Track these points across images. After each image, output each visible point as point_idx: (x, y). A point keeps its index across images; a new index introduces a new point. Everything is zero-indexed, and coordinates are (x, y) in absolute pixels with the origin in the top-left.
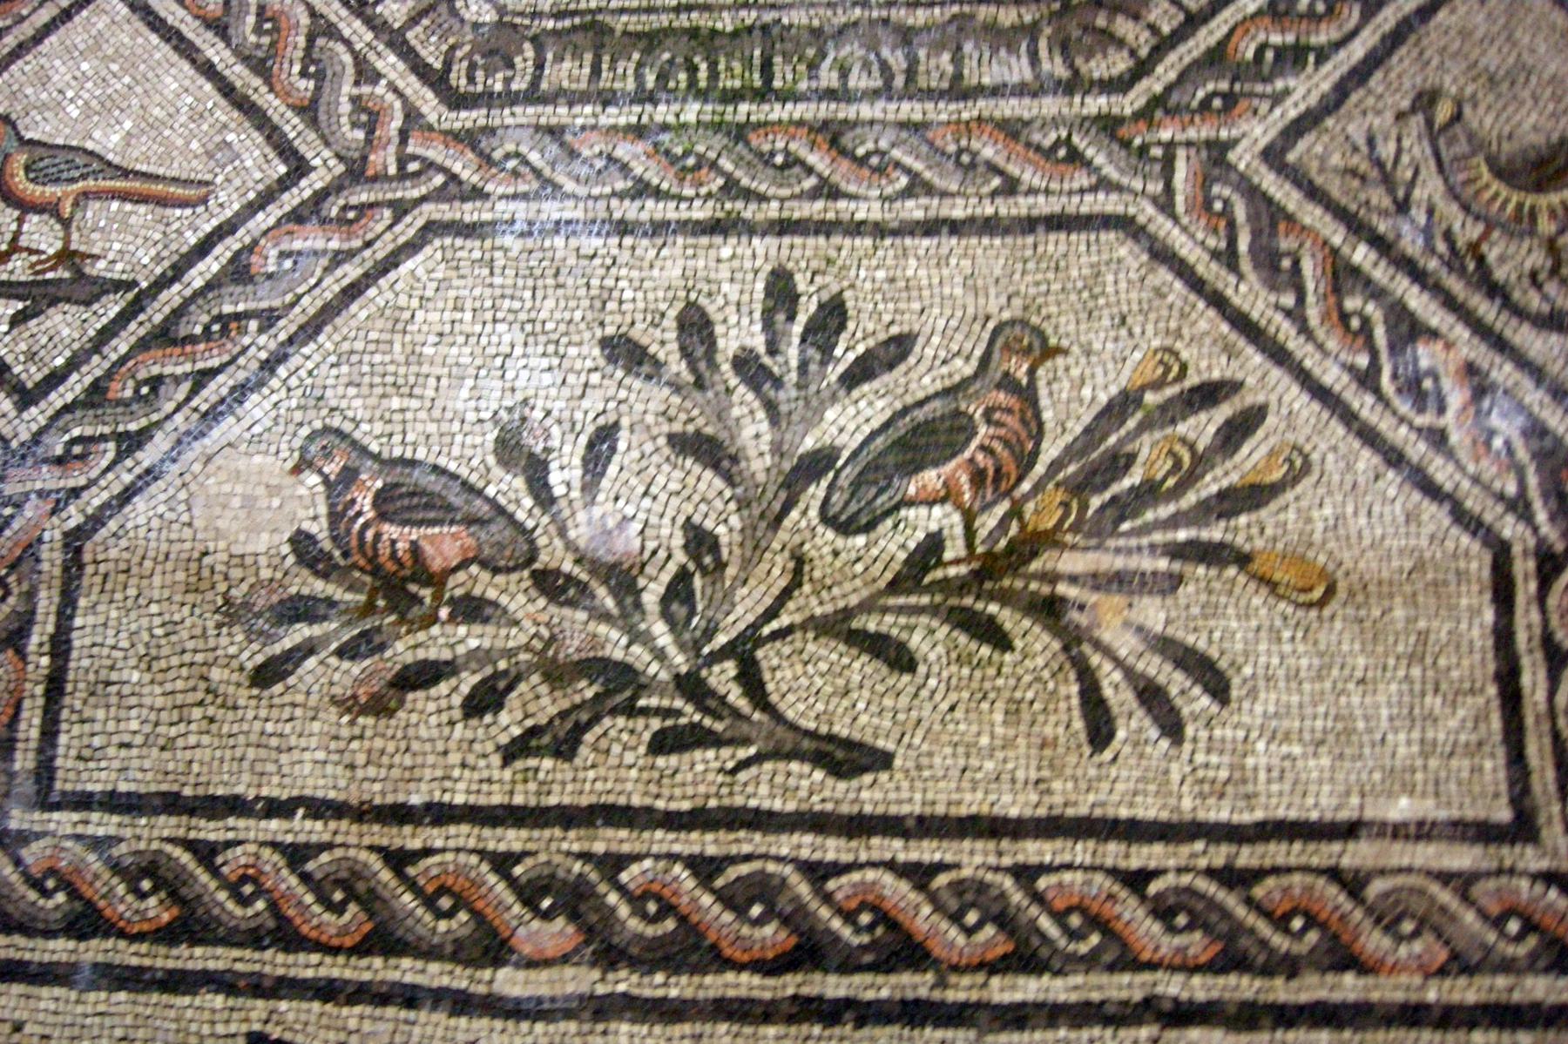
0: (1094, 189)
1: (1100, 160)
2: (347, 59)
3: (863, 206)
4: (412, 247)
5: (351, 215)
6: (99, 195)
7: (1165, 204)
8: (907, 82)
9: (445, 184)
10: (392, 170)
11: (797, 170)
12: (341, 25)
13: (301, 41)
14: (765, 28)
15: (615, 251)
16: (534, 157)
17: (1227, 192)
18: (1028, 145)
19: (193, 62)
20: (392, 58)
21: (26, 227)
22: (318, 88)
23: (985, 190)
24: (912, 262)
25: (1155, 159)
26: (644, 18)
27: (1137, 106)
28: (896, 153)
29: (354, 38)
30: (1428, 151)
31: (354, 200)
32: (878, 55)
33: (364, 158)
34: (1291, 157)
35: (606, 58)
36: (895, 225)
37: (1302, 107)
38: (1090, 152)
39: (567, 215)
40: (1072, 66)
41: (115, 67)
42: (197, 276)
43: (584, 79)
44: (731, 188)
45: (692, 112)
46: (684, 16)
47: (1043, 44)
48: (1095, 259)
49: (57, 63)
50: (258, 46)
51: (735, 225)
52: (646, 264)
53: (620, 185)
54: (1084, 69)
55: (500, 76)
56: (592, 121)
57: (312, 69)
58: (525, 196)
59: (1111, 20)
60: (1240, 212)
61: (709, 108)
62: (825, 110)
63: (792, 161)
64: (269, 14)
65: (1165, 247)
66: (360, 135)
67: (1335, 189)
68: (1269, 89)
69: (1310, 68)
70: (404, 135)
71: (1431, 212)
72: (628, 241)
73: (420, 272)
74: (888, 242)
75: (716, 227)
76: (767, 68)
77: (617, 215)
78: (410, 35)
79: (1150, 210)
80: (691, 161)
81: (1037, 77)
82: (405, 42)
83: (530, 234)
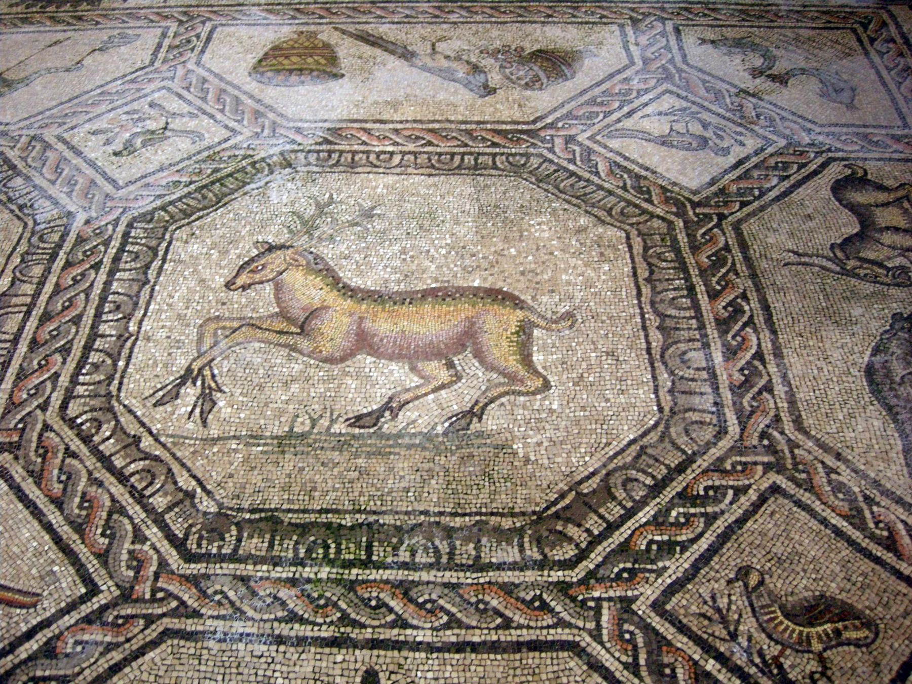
0: (554, 626)
1: (558, 609)
2: (129, 528)
3: (421, 633)
4: (154, 644)
5: (120, 621)
7: (596, 636)
8: (450, 559)
9: (177, 608)
10: (148, 596)
11: (383, 610)
12: (128, 508)
13: (104, 515)
14: (369, 525)
15: (274, 654)
16: (231, 594)
17: (632, 628)
18: (517, 599)
19: (40, 521)
20: (155, 530)
22: (110, 544)
23: (492, 625)
24: (449, 668)
25: (591, 608)
26: (301, 516)
27: (580, 577)
28: (441, 602)
29: (135, 516)
30: (746, 603)
31: (123, 613)
32: (433, 544)
33: (132, 588)
34: (668, 607)
35: (278, 538)
36: (439, 645)
37: (674, 577)
38: (553, 604)
39: (248, 630)
40: (543, 553)
42: (23, 652)
43: (264, 549)
44: (345, 619)
45: (325, 572)
46: (324, 516)
47: (526, 539)
48: (556, 668)
50: (79, 516)
51: (345, 642)
52: (292, 663)
53: (280, 614)
54: (550, 554)
55: (216, 544)
56: (267, 574)
57: (108, 532)
58: (223, 618)
59: (565, 527)
60: (640, 641)
61: (334, 570)
62: (401, 575)
63: (382, 605)
64: (88, 498)
65: (598, 661)
66: (131, 573)
67: (695, 625)
68: (655, 567)
69: (677, 556)
70: (157, 576)
71: (750, 639)
72: (282, 648)
73: (157, 660)
74: (435, 655)
75: (334, 643)
76: (369, 548)
77: (277, 632)
78: (167, 517)
79: (588, 639)
80: (322, 602)
81: (523, 559)
82: (164, 520)
83: (225, 640)
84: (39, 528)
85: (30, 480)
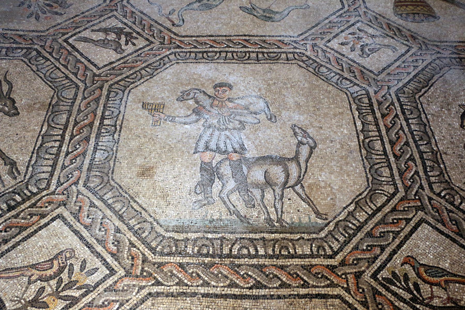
6: (451, 281)
19: (458, 244)
21: (434, 290)
41: (436, 244)
49: (419, 242)
84: (459, 247)
85: (439, 224)
